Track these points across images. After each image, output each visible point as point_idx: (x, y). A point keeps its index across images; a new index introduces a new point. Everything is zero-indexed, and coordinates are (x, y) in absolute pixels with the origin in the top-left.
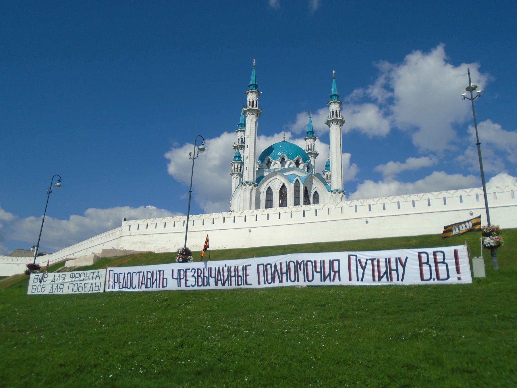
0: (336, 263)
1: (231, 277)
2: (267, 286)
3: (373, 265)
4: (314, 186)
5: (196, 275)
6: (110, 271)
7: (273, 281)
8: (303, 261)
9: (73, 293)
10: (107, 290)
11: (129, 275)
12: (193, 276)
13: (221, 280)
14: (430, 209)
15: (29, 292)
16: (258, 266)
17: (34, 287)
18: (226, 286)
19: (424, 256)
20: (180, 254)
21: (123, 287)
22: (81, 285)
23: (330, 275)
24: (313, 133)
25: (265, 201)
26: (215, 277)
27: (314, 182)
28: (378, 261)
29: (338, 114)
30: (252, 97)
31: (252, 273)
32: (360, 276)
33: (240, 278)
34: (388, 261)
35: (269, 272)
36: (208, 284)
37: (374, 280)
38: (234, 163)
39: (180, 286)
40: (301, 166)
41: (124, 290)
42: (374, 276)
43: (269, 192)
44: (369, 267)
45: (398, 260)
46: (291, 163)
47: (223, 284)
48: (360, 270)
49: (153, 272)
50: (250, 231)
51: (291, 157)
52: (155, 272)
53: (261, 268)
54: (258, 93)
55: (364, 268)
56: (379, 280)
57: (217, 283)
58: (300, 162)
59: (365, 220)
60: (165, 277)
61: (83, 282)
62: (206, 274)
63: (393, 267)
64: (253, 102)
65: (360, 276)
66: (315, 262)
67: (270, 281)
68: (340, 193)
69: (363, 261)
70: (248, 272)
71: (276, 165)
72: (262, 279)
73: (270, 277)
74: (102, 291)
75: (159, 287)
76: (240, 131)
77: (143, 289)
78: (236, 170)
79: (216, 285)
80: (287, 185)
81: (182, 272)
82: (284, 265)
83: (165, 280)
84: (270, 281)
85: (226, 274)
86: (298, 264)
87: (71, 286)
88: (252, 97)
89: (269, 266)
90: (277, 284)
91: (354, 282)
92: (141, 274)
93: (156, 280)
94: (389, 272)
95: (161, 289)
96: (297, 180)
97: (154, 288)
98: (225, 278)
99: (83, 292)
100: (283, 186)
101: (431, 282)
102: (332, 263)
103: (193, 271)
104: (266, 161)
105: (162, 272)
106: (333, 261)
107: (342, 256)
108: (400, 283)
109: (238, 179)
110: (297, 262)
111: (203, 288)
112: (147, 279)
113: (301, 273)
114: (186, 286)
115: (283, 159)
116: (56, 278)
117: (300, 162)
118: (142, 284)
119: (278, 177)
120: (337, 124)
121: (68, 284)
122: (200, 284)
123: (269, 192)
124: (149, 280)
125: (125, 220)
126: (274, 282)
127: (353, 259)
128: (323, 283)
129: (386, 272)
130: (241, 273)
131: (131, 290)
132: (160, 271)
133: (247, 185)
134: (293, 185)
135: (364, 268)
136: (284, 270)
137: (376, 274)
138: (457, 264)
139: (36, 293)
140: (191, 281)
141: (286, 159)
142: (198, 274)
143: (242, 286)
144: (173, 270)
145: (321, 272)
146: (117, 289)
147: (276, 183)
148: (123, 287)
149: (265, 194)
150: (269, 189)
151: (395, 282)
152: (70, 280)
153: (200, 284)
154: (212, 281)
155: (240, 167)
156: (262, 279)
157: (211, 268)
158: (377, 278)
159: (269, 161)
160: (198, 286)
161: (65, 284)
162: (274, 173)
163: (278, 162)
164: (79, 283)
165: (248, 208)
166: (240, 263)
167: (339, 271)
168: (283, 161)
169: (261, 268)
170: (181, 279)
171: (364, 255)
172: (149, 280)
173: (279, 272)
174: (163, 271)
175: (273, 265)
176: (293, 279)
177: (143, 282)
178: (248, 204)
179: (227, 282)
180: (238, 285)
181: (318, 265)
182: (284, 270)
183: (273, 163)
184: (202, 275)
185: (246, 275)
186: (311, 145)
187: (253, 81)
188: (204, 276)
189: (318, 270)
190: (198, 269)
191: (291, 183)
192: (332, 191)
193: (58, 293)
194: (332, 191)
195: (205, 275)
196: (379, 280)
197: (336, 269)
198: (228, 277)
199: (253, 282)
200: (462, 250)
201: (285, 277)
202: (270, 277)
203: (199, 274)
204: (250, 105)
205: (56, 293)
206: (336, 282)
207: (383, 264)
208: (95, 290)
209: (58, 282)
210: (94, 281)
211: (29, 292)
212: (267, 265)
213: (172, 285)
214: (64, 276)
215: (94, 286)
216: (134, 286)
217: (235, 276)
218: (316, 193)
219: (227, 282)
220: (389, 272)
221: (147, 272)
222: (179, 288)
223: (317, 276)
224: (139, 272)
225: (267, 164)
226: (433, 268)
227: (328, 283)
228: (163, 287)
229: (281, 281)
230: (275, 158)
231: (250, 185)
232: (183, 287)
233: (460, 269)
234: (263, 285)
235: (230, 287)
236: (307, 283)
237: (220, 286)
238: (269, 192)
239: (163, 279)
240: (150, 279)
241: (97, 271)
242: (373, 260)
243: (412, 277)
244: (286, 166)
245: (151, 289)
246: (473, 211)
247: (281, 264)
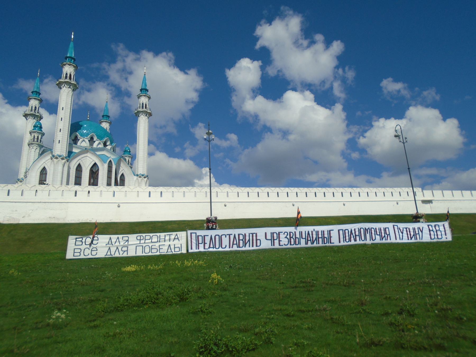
0: (387, 229)
1: (319, 238)
2: (346, 243)
3: (407, 231)
4: (121, 169)
5: (288, 237)
6: (191, 233)
7: (350, 240)
8: (369, 228)
9: (144, 254)
10: (190, 251)
11: (217, 237)
12: (286, 237)
13: (310, 240)
14: (269, 199)
15: (69, 255)
16: (339, 231)
17: (79, 251)
18: (315, 245)
19: (430, 227)
20: (213, 222)
21: (209, 247)
22: (153, 247)
23: (385, 236)
24: (109, 117)
25: (74, 177)
26: (305, 238)
27: (122, 164)
28: (409, 229)
30: (68, 69)
31: (335, 235)
32: (401, 237)
33: (325, 239)
34: (414, 229)
35: (347, 235)
36: (300, 243)
37: (408, 239)
38: (35, 132)
39: (274, 245)
40: (109, 147)
41: (211, 250)
42: (408, 237)
43: (79, 169)
44: (405, 232)
45: (419, 228)
46: (99, 144)
47: (313, 243)
48: (401, 234)
49: (245, 234)
50: (119, 206)
51: (100, 138)
52: (247, 235)
53: (341, 232)
54: (76, 67)
55: (402, 233)
56: (411, 239)
57: (307, 242)
58: (108, 143)
59: (223, 204)
60: (258, 238)
61: (157, 244)
62: (298, 236)
63: (417, 232)
64: (70, 75)
65: (401, 237)
66: (376, 229)
67: (347, 240)
68: (145, 178)
69: (402, 229)
70: (332, 235)
71: (84, 143)
72: (342, 239)
73: (347, 238)
74: (184, 251)
75: (253, 246)
76: (35, 99)
77: (235, 248)
78: (36, 140)
79: (307, 243)
80: (99, 164)
81: (275, 235)
82: (357, 230)
83: (258, 242)
84: (347, 240)
85: (314, 236)
86: (366, 230)
87: (139, 249)
88: (68, 69)
89: (347, 231)
90: (353, 242)
91: (398, 241)
92: (232, 237)
93: (249, 240)
94: (415, 235)
95: (255, 248)
96: (110, 161)
97: (247, 248)
98: (314, 239)
99: (158, 253)
100: (95, 164)
101: (435, 240)
102: (385, 229)
103: (286, 234)
104: (73, 137)
105: (254, 235)
106: (385, 228)
107: (390, 225)
108: (421, 241)
109: (38, 151)
110: (365, 228)
111: (295, 246)
112: (239, 240)
113: (368, 236)
114: (280, 245)
115: (92, 138)
116: (114, 240)
118: (233, 244)
119: (89, 155)
120: (146, 116)
121: (135, 246)
122: (292, 243)
123: (79, 169)
124: (241, 242)
126: (351, 241)
127: (396, 227)
128: (381, 242)
129: (414, 235)
130: (326, 235)
131: (220, 249)
132: (253, 234)
133: (60, 159)
134: (106, 166)
135: (402, 233)
136: (357, 233)
137: (409, 236)
138: (445, 231)
139: (82, 257)
140: (284, 241)
141: (95, 138)
142: (290, 237)
143: (327, 245)
144: (266, 233)
145: (380, 235)
146: (201, 249)
147: (87, 161)
148: (209, 247)
149: (75, 170)
151: (418, 240)
152: (138, 242)
153: (292, 243)
154: (303, 241)
155: (41, 138)
156: (342, 239)
157: (302, 232)
158: (410, 238)
159: (76, 137)
160: (291, 244)
161: (130, 247)
162: (85, 151)
163: (87, 141)
164: (150, 245)
165: (59, 183)
166: (326, 228)
167: (389, 234)
168: (92, 140)
169: (341, 232)
170: (274, 240)
171: (402, 226)
172: (241, 242)
173: (354, 235)
174: (256, 234)
175: (350, 230)
176: (363, 239)
177: (235, 243)
178: (59, 179)
179: (315, 242)
180: (324, 243)
181: (378, 231)
182: (357, 233)
183: (81, 140)
184: (294, 237)
185: (330, 237)
187: (71, 53)
188: (296, 238)
189: (378, 234)
190: (290, 233)
191: (105, 162)
192: (137, 175)
193: (121, 256)
194: (137, 175)
195: (297, 237)
196: (411, 239)
197: (388, 233)
198: (316, 238)
199: (335, 241)
200: (447, 224)
201: (358, 238)
202: (347, 238)
203: (292, 236)
204: (66, 77)
205: (117, 255)
206: (389, 241)
207: (412, 230)
208: (177, 251)
209: (117, 244)
210: (172, 243)
211: (69, 255)
212: (345, 230)
213: (266, 245)
214: (127, 239)
215: (172, 247)
216: (223, 246)
217: (322, 238)
218: (123, 175)
219: (315, 242)
220: (415, 235)
221: (239, 235)
222: (273, 247)
223: (378, 237)
224: (229, 235)
225: (73, 140)
226: (435, 233)
227: (384, 241)
228: (257, 246)
229: (355, 240)
230: (83, 135)
231: (63, 159)
232: (277, 246)
233: (444, 233)
234: (342, 243)
235: (318, 245)
236: (372, 242)
237: (309, 244)
238: (79, 169)
239: (257, 240)
240: (242, 240)
241: (174, 233)
242: (406, 228)
243: (426, 238)
244: (95, 145)
245: (244, 249)
246: (294, 203)
247: (355, 230)
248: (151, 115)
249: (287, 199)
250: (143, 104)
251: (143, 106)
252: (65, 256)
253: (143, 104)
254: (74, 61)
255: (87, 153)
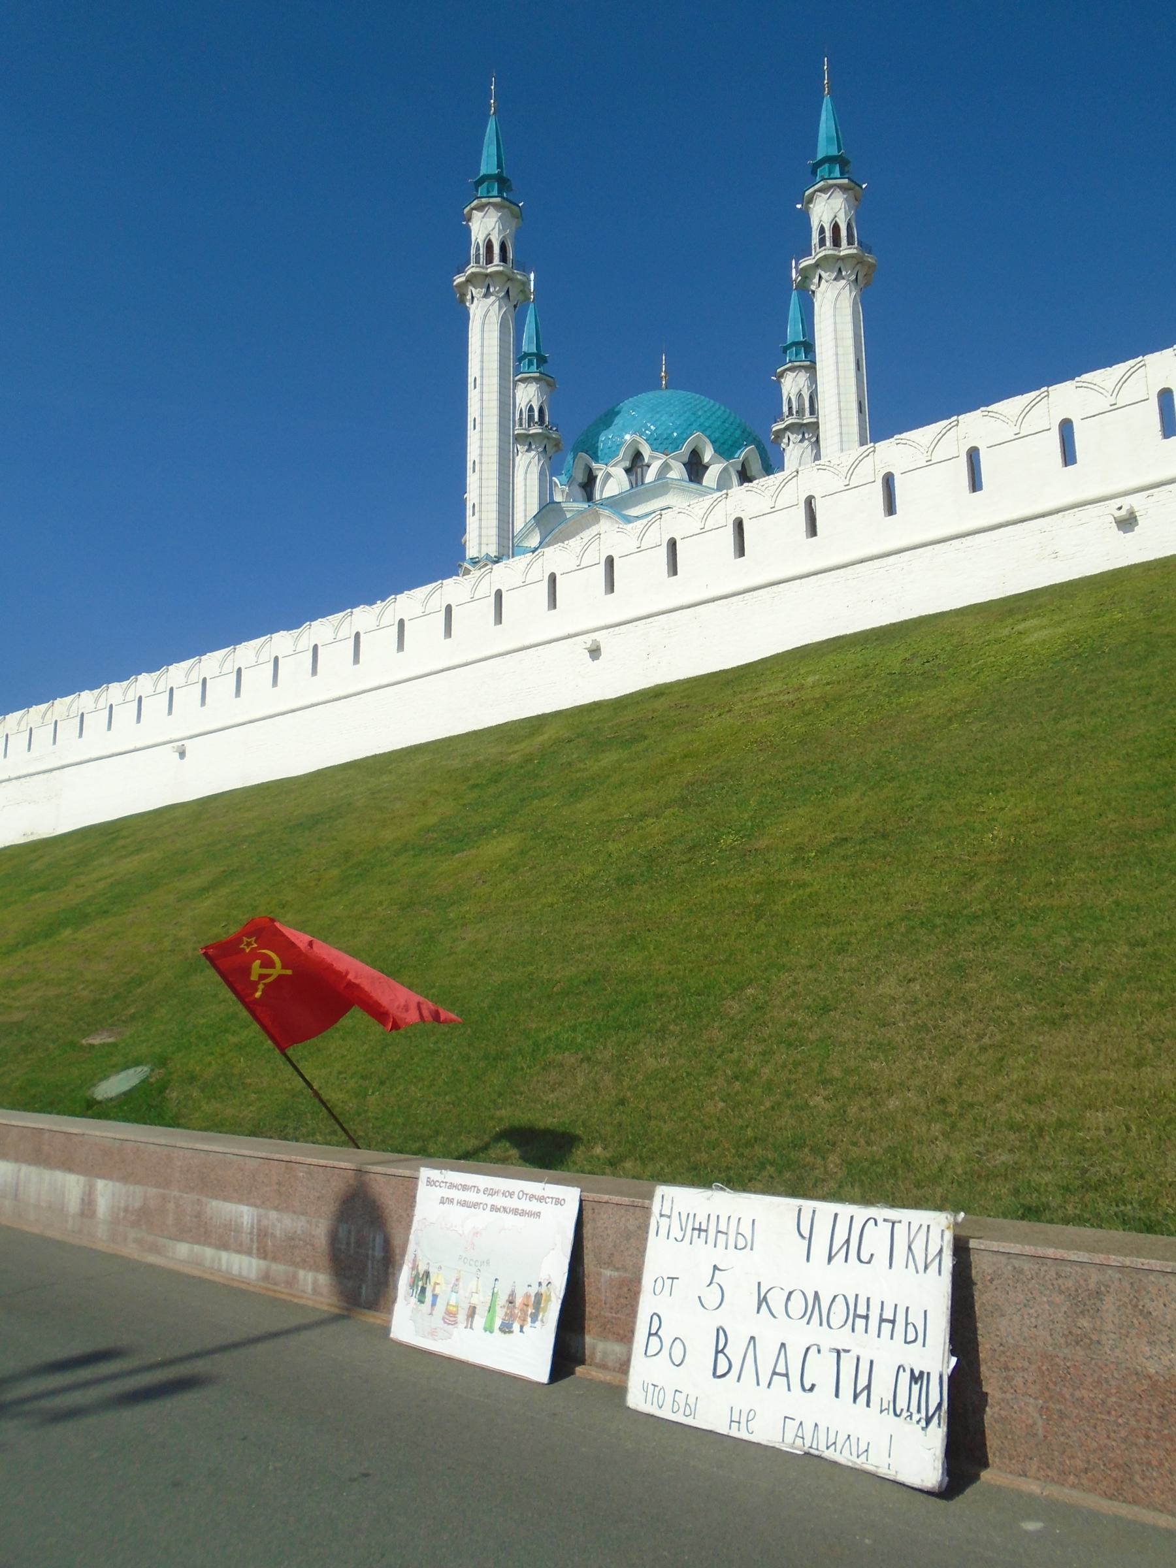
29: (844, 233)
46: (666, 467)
51: (663, 444)
58: (708, 455)
104: (580, 477)
115: (638, 456)
117: (706, 459)
168: (635, 465)
186: (800, 395)
246: (1136, 502)
249: (1068, 485)
255: (597, 521)
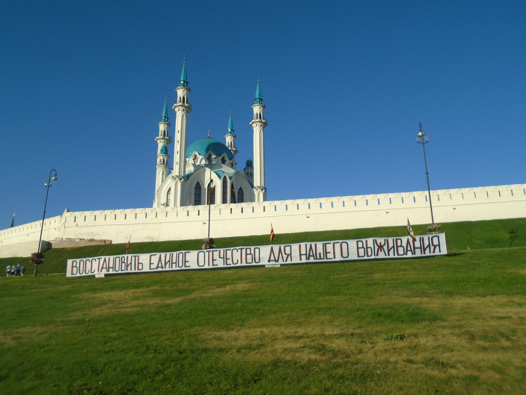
51: (218, 155)
58: (226, 158)
59: (305, 216)
125: (68, 211)
150: (198, 183)
204: (180, 102)
218: (241, 189)
225: (193, 159)
248: (267, 125)
249: (378, 207)
250: (257, 114)
251: (257, 116)
252: (66, 275)
253: (257, 114)
254: (186, 84)
